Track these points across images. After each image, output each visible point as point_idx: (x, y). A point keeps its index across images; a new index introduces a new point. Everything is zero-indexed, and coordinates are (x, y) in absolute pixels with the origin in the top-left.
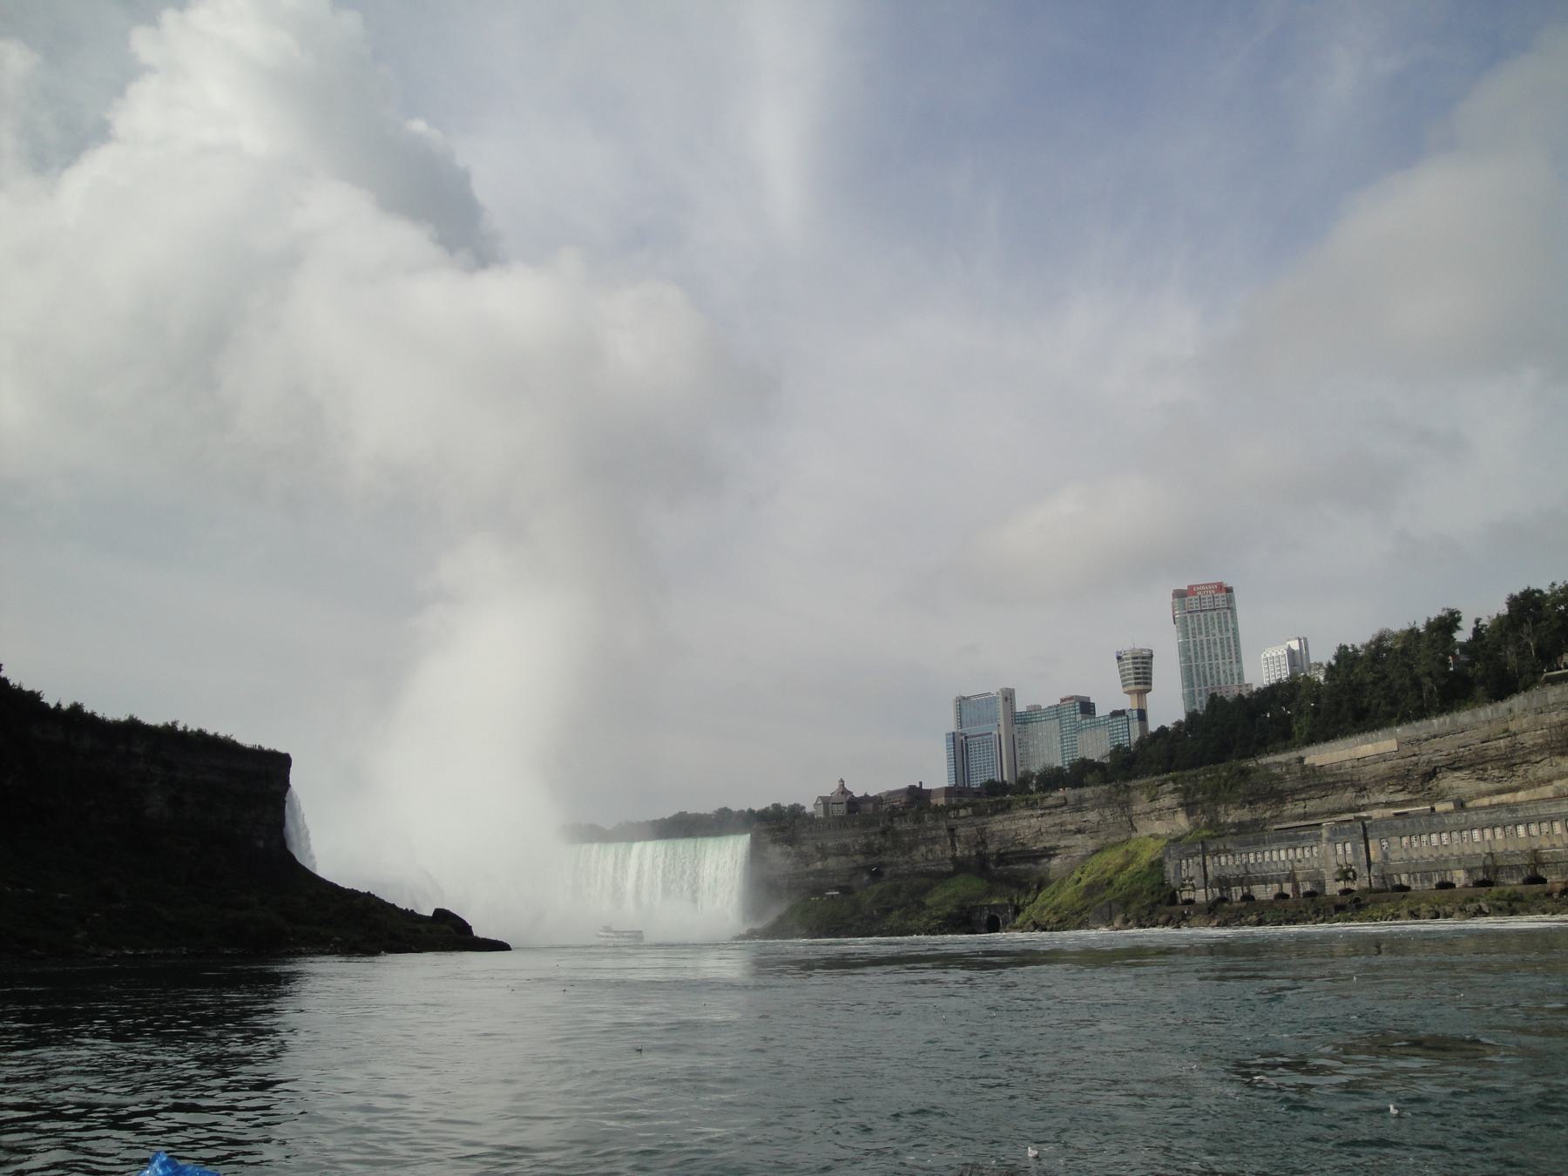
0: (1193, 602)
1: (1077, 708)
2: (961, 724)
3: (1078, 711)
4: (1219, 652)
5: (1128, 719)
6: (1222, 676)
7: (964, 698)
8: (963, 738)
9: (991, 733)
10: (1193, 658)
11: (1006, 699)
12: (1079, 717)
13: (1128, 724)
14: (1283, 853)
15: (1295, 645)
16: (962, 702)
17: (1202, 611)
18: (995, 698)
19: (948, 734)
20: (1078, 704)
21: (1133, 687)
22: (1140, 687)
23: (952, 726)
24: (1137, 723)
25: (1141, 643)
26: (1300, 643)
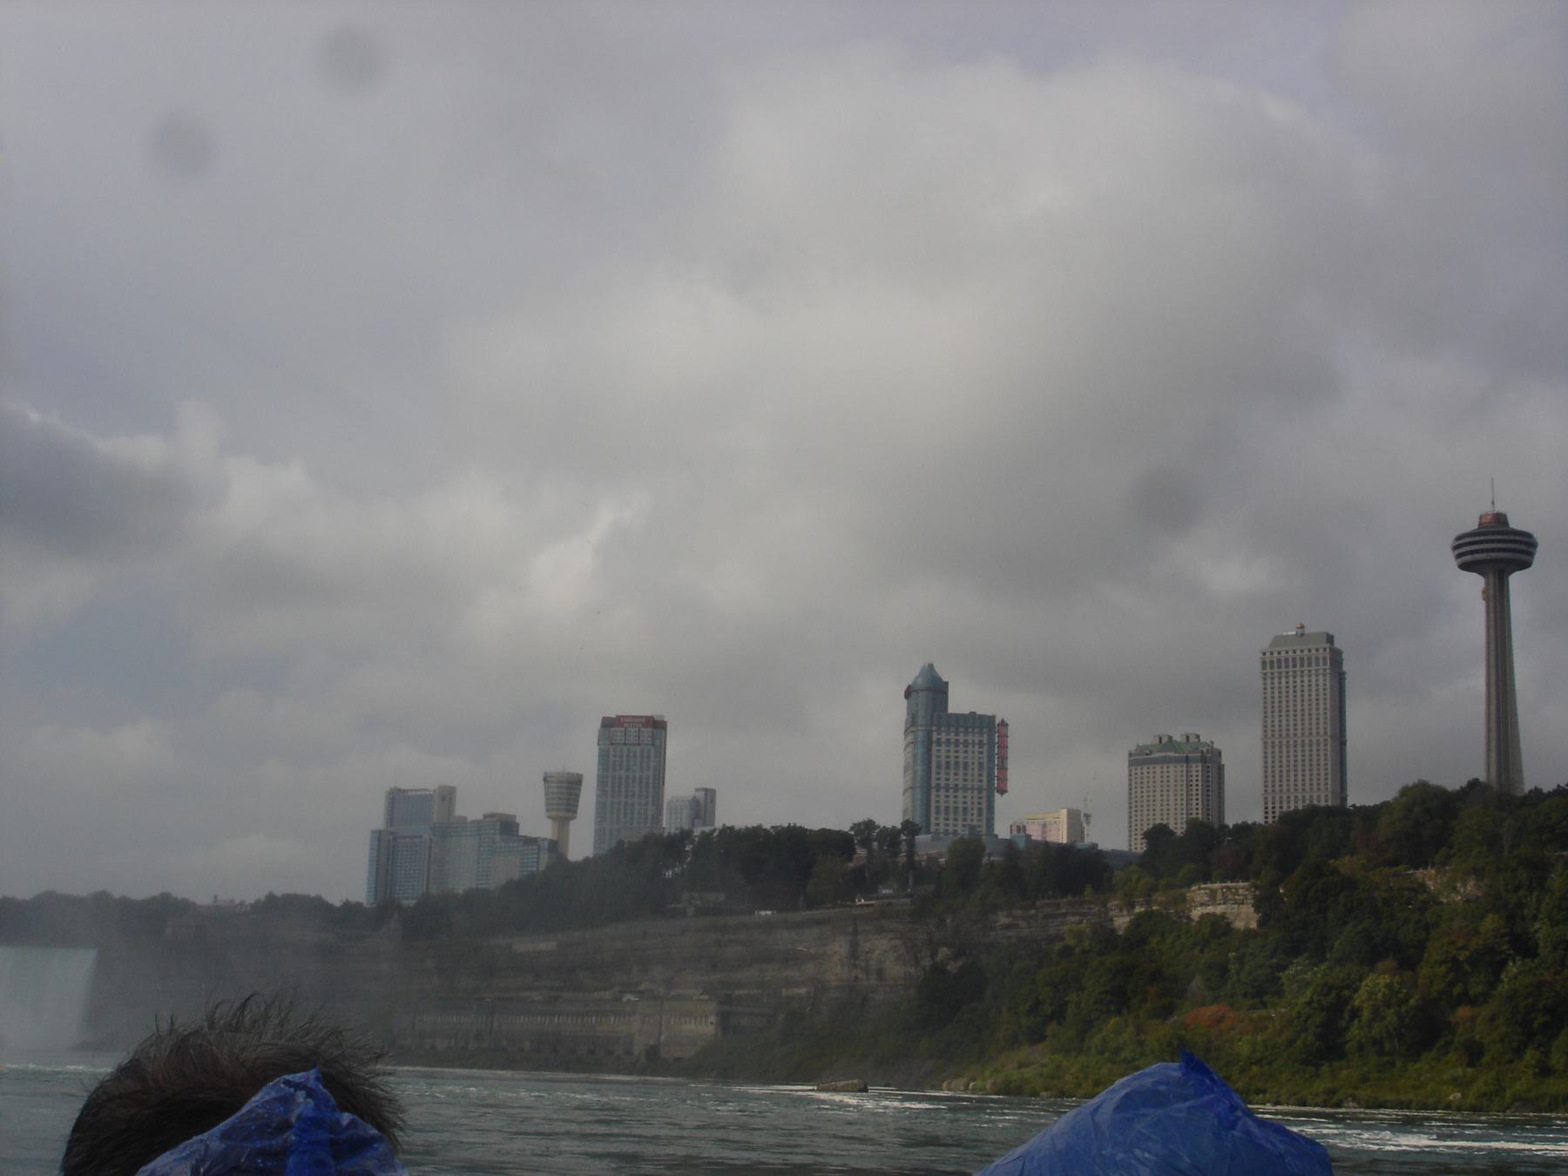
0: (619, 734)
1: (498, 827)
2: (391, 817)
3: (498, 832)
4: (637, 790)
5: (539, 850)
6: (636, 816)
7: (399, 790)
8: (391, 837)
9: (421, 837)
10: (609, 793)
11: (443, 799)
12: (498, 838)
13: (538, 854)
14: (455, 1018)
15: (701, 795)
16: (396, 799)
17: (625, 744)
18: (431, 795)
19: (373, 832)
20: (498, 823)
21: (553, 814)
22: (562, 814)
23: (380, 824)
24: (546, 856)
25: (574, 768)
26: (706, 795)
